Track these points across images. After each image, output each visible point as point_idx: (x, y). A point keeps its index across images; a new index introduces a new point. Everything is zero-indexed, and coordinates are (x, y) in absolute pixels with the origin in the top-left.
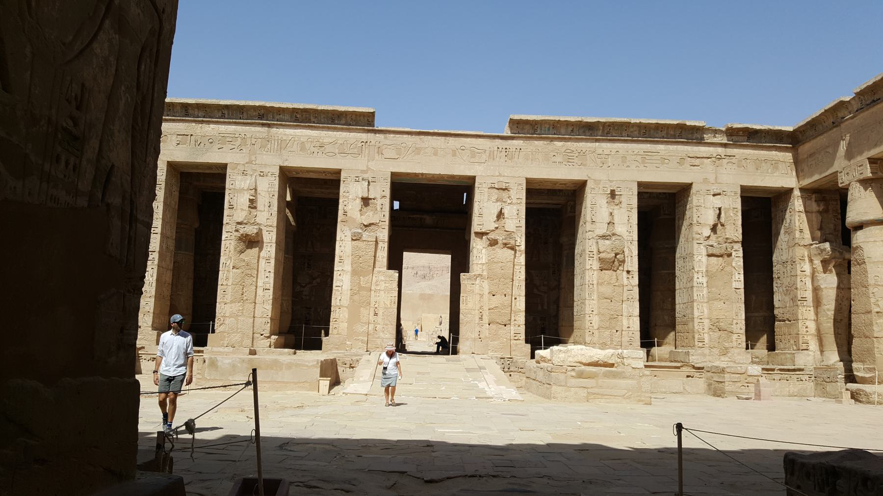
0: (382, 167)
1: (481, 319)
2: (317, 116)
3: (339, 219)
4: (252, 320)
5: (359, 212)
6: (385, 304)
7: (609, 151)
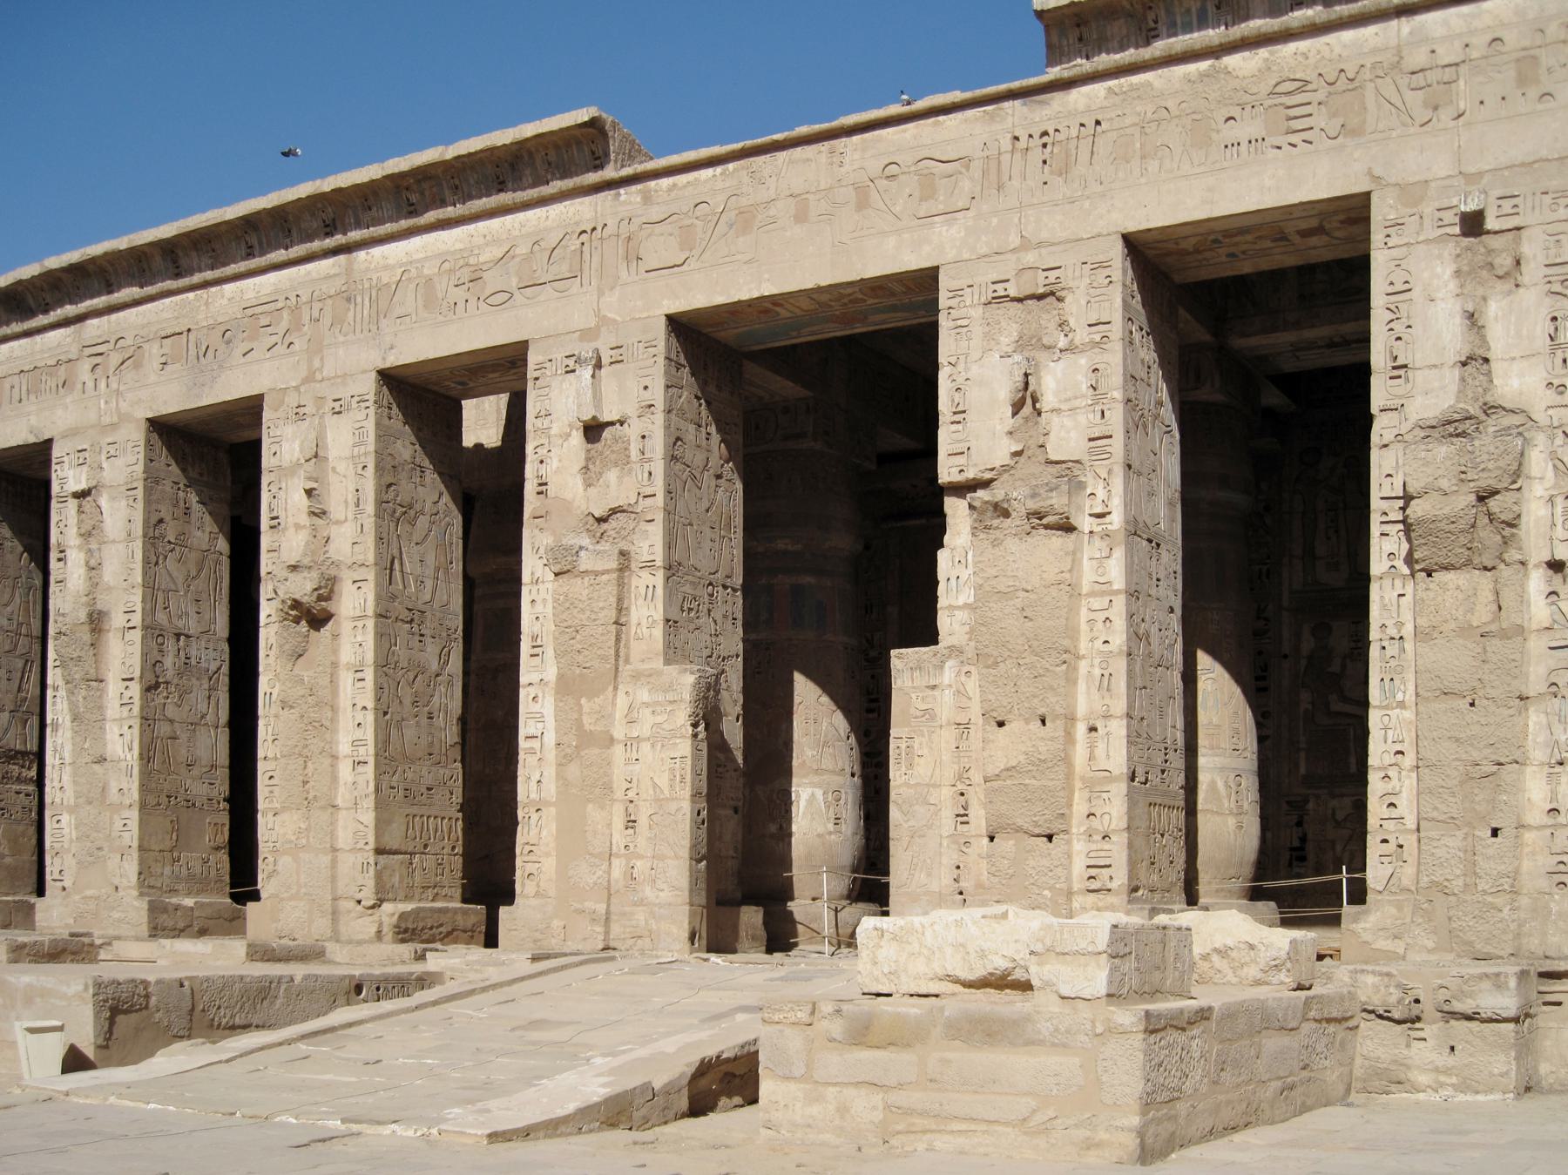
0: (639, 303)
1: (962, 817)
2: (457, 182)
4: (329, 857)
6: (655, 785)
7: (1458, 45)
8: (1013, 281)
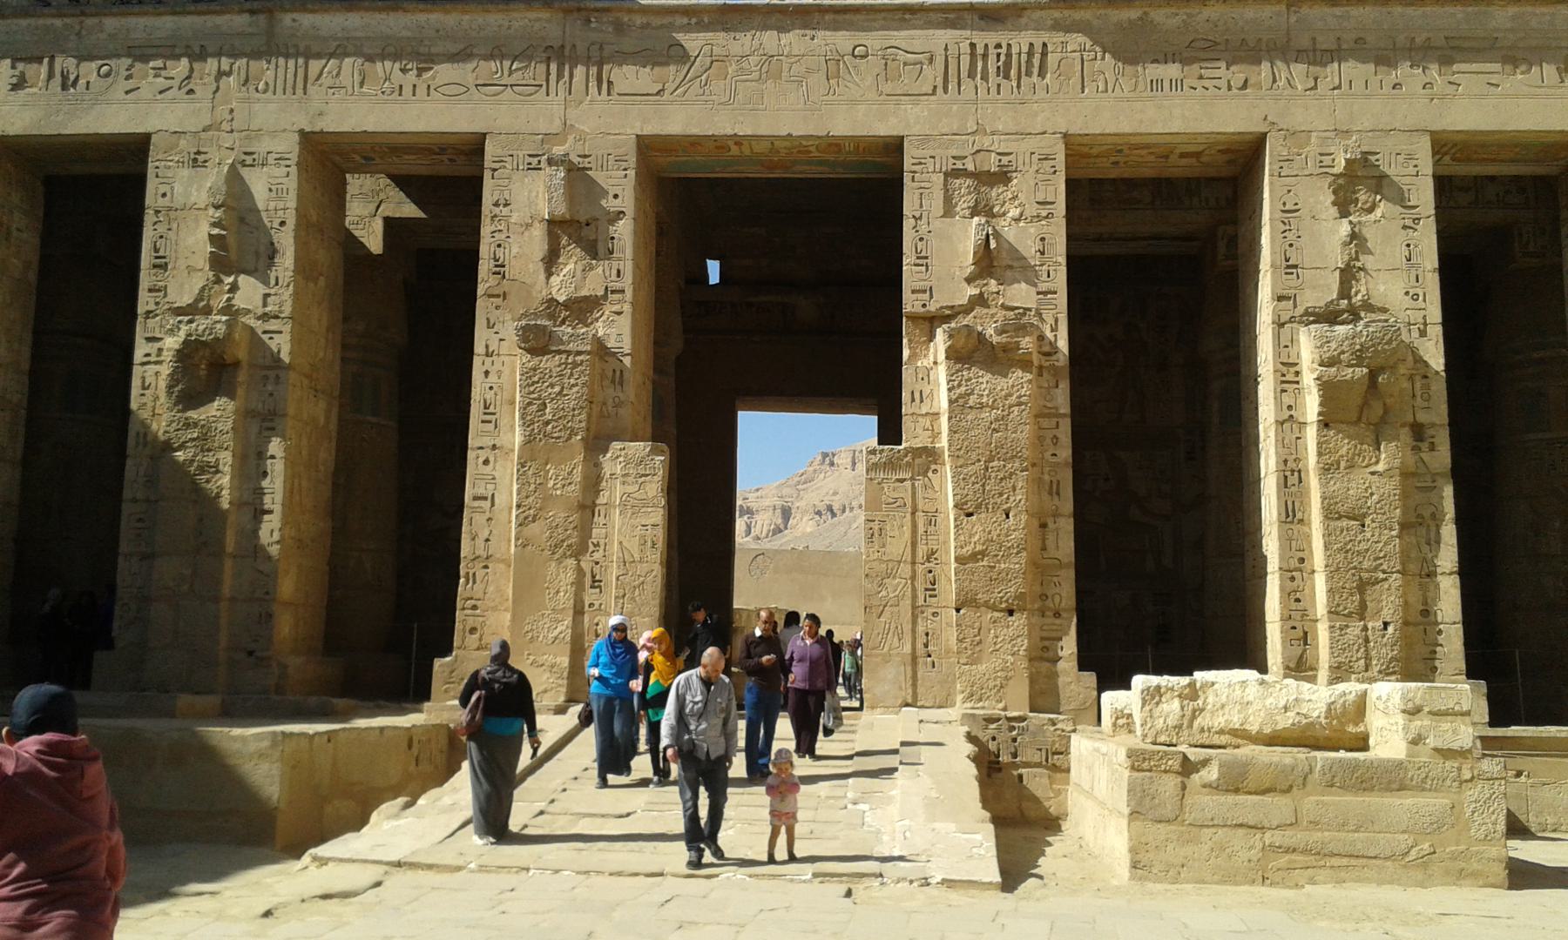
1: (931, 590)
3: (481, 289)
5: (541, 263)
8: (970, 158)
